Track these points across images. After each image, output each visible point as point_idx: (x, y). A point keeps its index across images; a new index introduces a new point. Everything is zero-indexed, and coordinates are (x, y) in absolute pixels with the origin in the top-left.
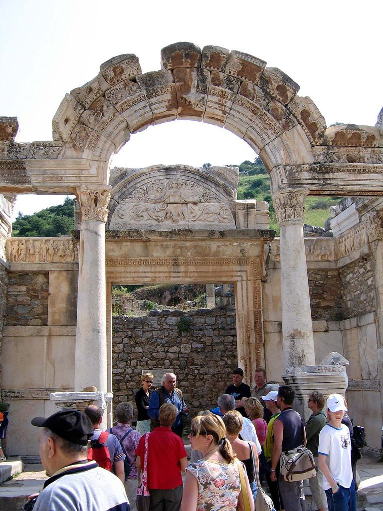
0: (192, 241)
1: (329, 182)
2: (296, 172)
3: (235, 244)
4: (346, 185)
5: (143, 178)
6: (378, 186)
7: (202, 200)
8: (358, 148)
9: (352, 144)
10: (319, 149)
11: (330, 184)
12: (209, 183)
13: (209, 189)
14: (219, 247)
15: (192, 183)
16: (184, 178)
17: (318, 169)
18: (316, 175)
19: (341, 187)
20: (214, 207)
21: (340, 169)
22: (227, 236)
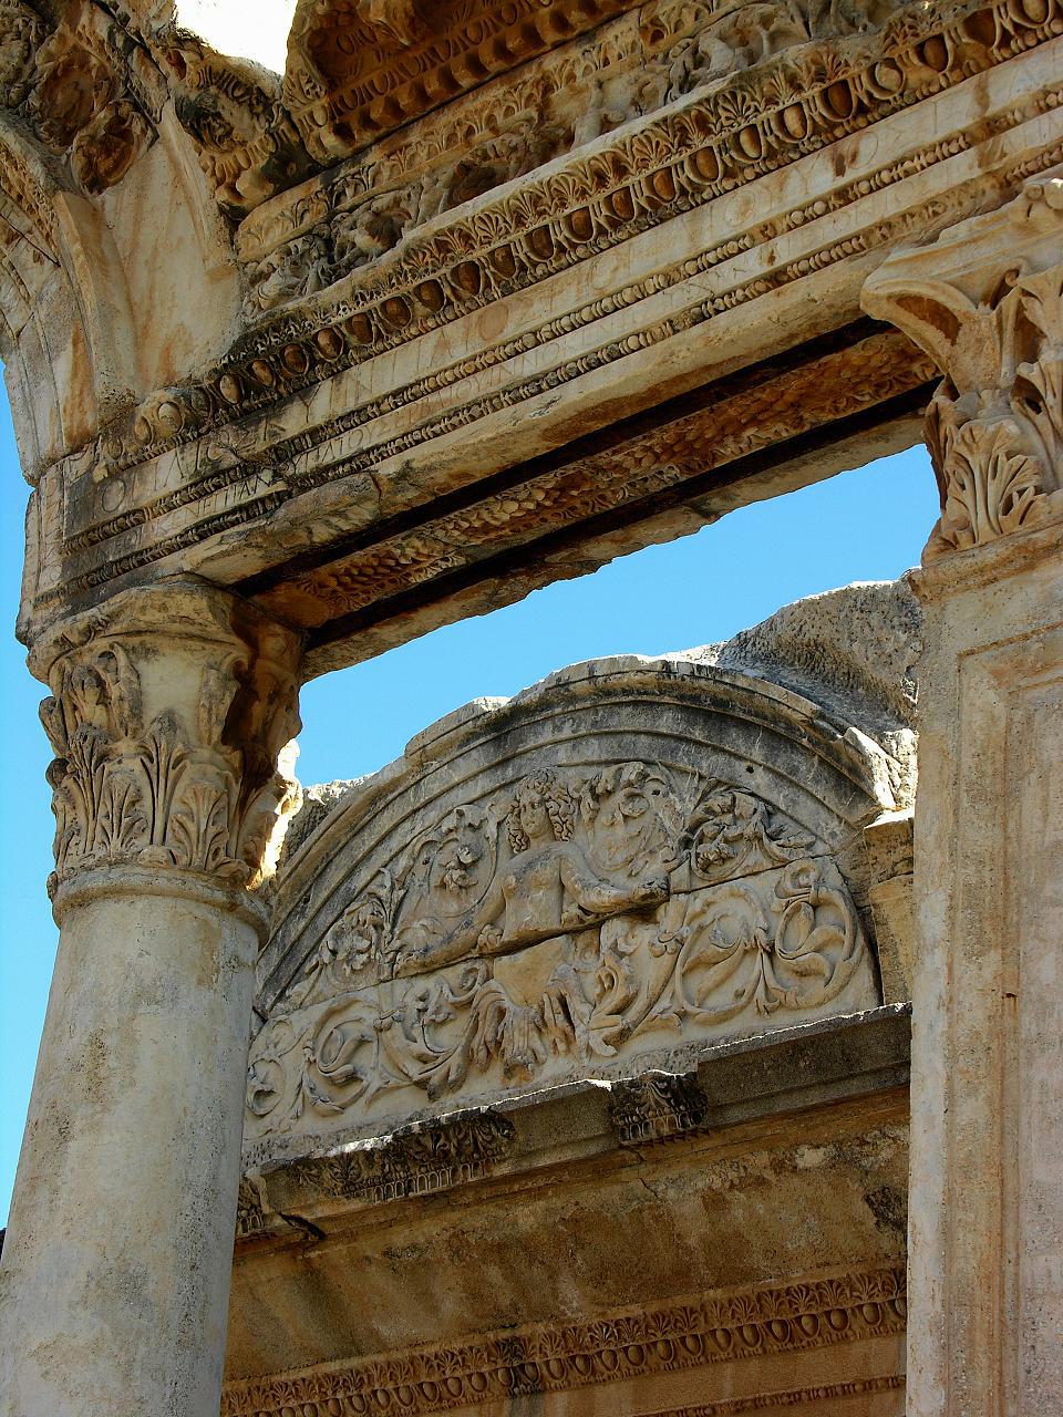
0: (539, 1193)
1: (305, 464)
2: (113, 476)
3: (810, 1158)
4: (430, 429)
5: (385, 822)
6: (673, 326)
7: (680, 877)
8: (530, 75)
9: (476, 66)
10: (275, 223)
11: (321, 475)
12: (735, 740)
13: (731, 786)
14: (714, 1202)
15: (631, 772)
16: (594, 750)
17: (228, 390)
18: (226, 446)
19: (389, 467)
20: (743, 905)
21: (366, 316)
22: (722, 1107)
